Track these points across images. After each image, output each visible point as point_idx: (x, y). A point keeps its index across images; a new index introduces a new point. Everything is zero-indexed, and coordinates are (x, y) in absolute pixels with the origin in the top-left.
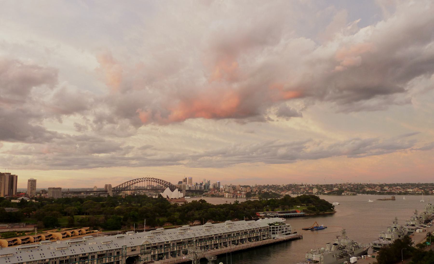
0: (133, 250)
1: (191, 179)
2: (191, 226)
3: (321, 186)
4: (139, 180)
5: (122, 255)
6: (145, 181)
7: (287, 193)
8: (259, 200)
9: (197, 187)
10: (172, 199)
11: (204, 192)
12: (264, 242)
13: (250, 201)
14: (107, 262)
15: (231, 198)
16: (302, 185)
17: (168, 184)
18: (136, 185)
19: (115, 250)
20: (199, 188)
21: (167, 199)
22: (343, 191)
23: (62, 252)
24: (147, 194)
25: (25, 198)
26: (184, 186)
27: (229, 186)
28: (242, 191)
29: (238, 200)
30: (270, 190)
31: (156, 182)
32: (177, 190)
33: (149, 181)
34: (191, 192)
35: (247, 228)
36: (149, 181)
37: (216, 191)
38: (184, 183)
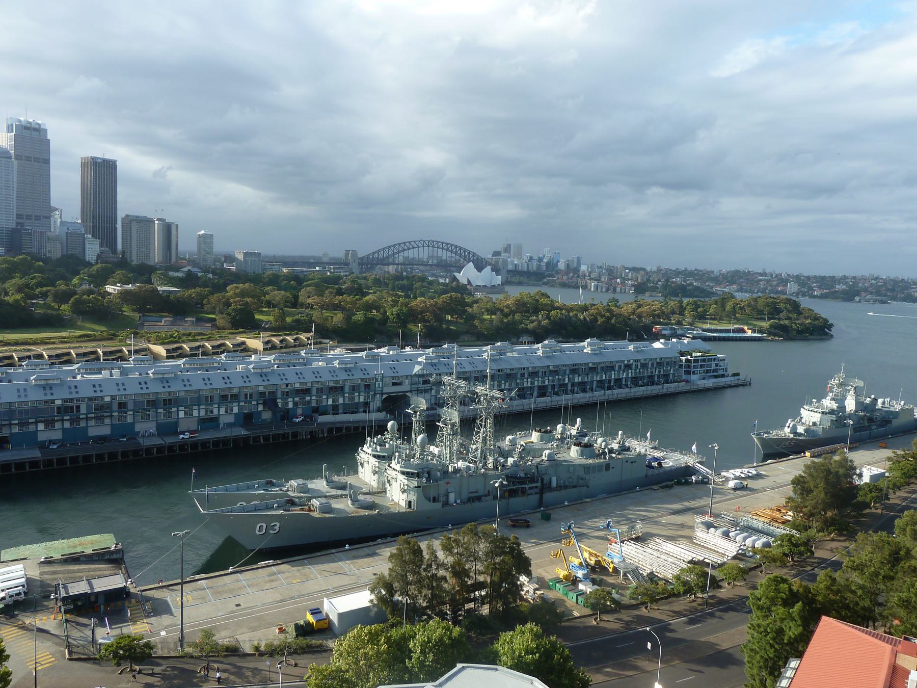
1: (519, 248)
3: (808, 278)
4: (412, 243)
6: (423, 246)
7: (726, 290)
9: (532, 266)
10: (477, 286)
11: (545, 277)
15: (602, 292)
16: (764, 274)
17: (471, 256)
20: (535, 268)
21: (469, 287)
22: (858, 293)
26: (505, 262)
27: (601, 267)
28: (628, 279)
29: (617, 296)
30: (688, 280)
31: (447, 250)
32: (489, 268)
34: (516, 276)
36: (433, 247)
37: (571, 275)
38: (504, 255)
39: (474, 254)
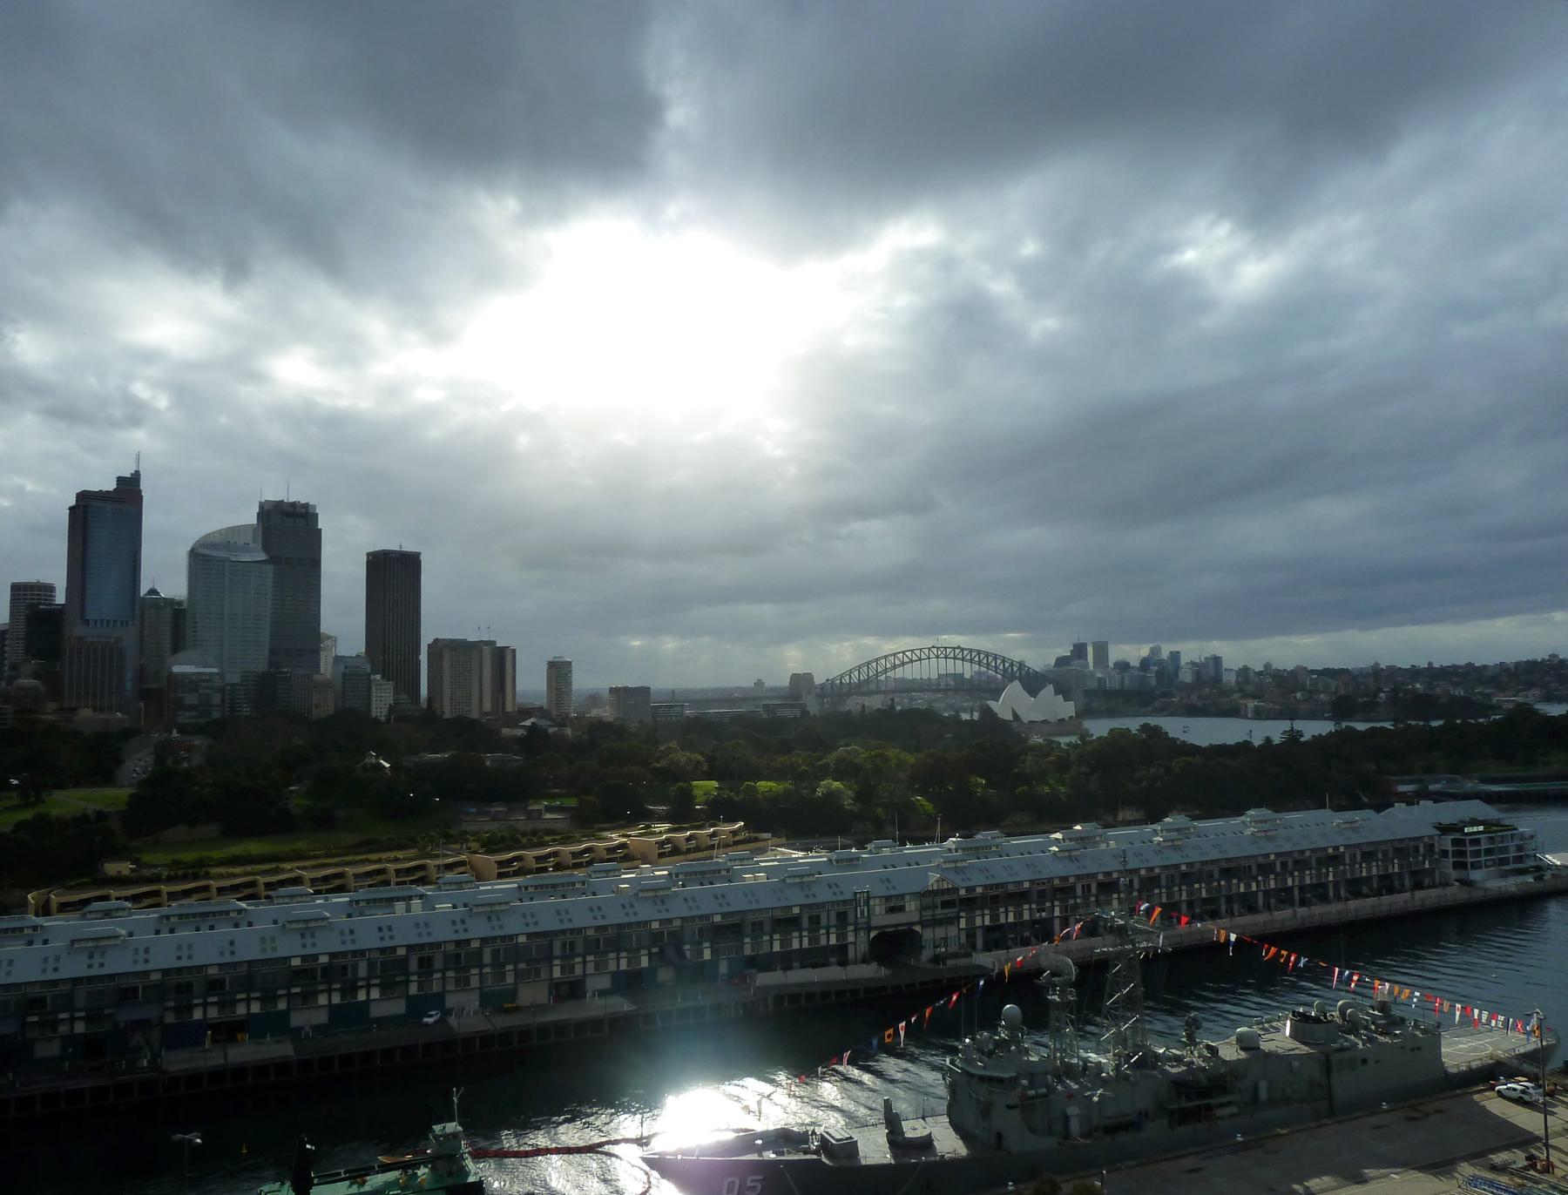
0: (892, 910)
1: (1101, 649)
2: (1106, 826)
5: (856, 924)
6: (929, 658)
8: (1392, 728)
10: (1031, 722)
12: (1417, 898)
13: (1351, 730)
14: (806, 944)
17: (1015, 669)
18: (899, 673)
19: (833, 903)
21: (1015, 725)
23: (656, 905)
24: (938, 706)
25: (543, 723)
27: (1261, 673)
28: (1319, 692)
31: (971, 661)
32: (1050, 688)
33: (946, 657)
34: (1103, 699)
35: (1340, 841)
36: (946, 657)
39: (1021, 664)
